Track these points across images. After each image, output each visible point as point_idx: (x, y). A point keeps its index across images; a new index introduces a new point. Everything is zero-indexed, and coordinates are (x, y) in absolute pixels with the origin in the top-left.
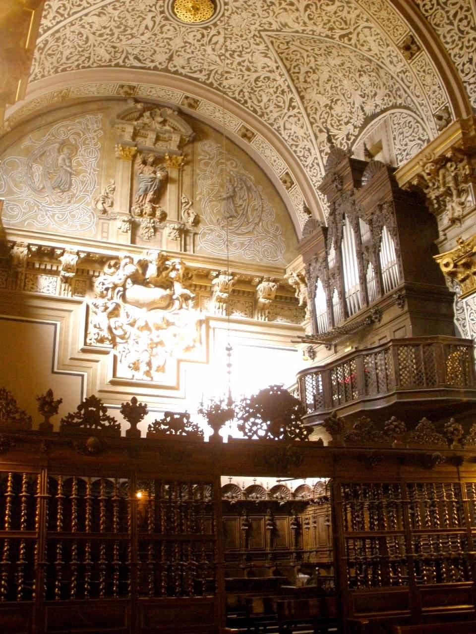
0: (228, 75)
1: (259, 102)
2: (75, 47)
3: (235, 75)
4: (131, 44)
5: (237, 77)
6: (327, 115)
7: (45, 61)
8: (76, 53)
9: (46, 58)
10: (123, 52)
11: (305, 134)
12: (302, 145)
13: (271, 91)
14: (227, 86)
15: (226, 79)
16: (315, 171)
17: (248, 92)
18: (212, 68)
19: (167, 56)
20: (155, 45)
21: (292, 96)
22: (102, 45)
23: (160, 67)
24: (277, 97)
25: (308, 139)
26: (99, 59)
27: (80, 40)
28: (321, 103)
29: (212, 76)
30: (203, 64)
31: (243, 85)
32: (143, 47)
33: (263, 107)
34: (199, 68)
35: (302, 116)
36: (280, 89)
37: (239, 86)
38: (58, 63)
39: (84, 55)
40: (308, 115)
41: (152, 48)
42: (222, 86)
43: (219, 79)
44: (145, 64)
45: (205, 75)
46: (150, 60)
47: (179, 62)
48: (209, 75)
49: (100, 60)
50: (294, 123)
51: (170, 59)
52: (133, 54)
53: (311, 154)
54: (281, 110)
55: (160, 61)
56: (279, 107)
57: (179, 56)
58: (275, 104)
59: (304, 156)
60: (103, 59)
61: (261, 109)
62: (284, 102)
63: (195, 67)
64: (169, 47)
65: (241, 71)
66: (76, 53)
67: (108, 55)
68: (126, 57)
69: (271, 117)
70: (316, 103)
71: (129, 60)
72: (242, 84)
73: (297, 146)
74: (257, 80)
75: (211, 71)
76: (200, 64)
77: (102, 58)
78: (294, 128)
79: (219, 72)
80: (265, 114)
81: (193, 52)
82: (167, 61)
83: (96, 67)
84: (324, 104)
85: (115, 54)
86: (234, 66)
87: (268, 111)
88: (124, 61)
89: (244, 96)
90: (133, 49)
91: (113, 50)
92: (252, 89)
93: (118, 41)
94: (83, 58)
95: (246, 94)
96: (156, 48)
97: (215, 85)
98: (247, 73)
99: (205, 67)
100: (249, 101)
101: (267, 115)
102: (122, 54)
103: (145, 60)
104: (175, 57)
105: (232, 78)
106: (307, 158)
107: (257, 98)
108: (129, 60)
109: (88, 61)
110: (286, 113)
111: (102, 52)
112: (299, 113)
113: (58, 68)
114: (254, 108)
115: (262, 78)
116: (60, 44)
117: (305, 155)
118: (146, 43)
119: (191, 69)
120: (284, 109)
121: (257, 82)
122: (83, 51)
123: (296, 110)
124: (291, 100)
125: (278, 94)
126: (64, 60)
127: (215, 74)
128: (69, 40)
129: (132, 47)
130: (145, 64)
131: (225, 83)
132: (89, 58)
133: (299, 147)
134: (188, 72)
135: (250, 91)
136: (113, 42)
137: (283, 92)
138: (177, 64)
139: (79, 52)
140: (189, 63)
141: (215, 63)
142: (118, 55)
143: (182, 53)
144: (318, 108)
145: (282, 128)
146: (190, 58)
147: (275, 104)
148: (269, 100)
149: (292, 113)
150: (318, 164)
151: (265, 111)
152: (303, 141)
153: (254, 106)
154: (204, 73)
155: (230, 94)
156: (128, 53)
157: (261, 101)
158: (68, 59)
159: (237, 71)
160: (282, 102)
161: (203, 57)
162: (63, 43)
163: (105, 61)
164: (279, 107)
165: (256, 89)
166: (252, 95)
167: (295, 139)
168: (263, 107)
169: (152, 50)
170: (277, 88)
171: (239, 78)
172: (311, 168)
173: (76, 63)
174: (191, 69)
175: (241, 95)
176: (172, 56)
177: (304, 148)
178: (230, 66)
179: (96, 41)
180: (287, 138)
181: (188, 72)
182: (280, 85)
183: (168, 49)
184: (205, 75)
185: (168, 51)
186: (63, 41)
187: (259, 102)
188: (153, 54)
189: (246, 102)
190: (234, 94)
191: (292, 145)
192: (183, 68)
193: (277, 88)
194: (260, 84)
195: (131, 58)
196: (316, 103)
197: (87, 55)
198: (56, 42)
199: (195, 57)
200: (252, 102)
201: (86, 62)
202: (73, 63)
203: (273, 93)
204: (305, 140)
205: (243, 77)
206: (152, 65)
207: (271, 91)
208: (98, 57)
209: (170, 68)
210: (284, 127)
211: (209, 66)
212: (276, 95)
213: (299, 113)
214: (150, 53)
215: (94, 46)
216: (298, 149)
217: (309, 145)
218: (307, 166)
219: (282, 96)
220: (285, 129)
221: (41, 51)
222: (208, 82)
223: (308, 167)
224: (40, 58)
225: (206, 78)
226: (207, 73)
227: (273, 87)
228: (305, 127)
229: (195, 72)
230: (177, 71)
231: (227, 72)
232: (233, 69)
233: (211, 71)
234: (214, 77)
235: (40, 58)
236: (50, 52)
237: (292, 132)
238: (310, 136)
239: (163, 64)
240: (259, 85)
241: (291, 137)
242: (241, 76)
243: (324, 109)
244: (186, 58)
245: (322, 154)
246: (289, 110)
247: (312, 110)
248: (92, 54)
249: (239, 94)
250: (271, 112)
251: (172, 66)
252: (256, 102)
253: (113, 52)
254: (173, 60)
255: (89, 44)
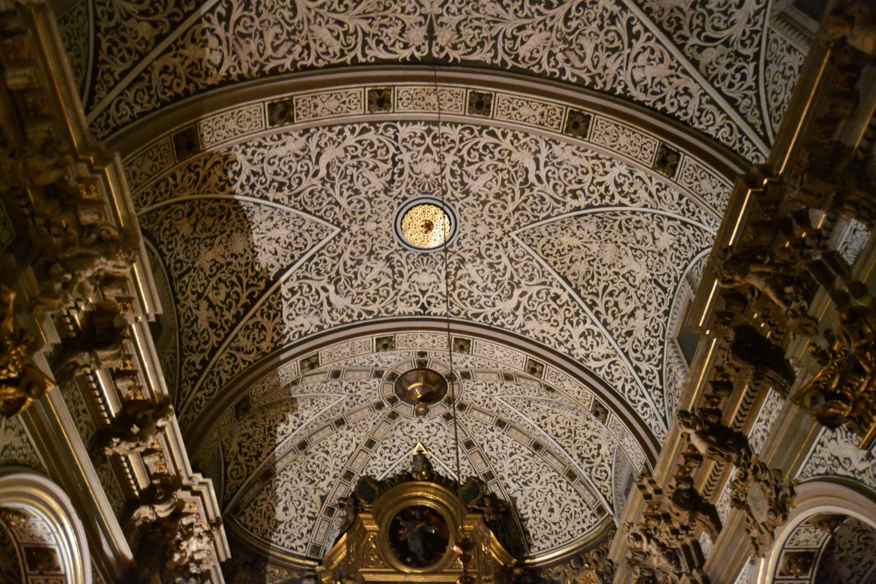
0: (523, 34)
1: (582, 60)
2: (279, 23)
3: (533, 28)
4: (364, 12)
5: (537, 30)
6: (701, 18)
7: (239, 50)
8: (285, 36)
9: (236, 40)
10: (356, 32)
11: (671, 67)
12: (669, 91)
13: (594, 26)
14: (528, 55)
15: (523, 43)
16: (710, 116)
17: (561, 51)
18: (494, 33)
19: (423, 31)
20: (400, 10)
21: (630, 15)
22: (319, 19)
23: (418, 55)
24: (606, 34)
25: (679, 73)
26: (323, 49)
27: (283, 7)
28: (683, 6)
29: (500, 47)
30: (480, 28)
31: (550, 42)
32: (384, 17)
33: (591, 67)
34: (478, 40)
35: (658, 41)
36: (606, 15)
37: (544, 47)
38: (261, 55)
39: (298, 42)
40: (669, 35)
41: (397, 18)
42: (520, 59)
43: (511, 49)
44: (395, 53)
45: (489, 51)
46: (402, 45)
47: (444, 36)
48: (495, 47)
49: (327, 53)
50: (644, 63)
51: (431, 37)
52: (374, 35)
53: (691, 95)
54: (620, 55)
55: (417, 44)
56: (614, 50)
57: (442, 24)
58: (608, 49)
59: (680, 108)
60: (331, 50)
61: (589, 71)
62: (620, 37)
63: (471, 40)
64: (423, 11)
65: (540, 13)
66: (285, 36)
67: (334, 41)
68: (365, 43)
69: (608, 80)
70: (675, 10)
71: (370, 48)
72: (548, 39)
73: (663, 100)
74: (567, 19)
75: (496, 38)
76: (478, 31)
77: (327, 48)
78: (650, 71)
79: (509, 35)
80: (597, 79)
81: (460, 10)
82: (427, 42)
83: (326, 67)
84: (689, 5)
85: (345, 39)
86: (526, 11)
87: (600, 70)
88: (364, 55)
89: (557, 63)
90: (370, 25)
91: (341, 29)
92: (565, 41)
93: (342, 9)
94: (298, 49)
95: (560, 57)
96: (402, 16)
97: (510, 63)
98: (551, 12)
99: (485, 33)
100: (567, 67)
101: (601, 77)
102: (356, 38)
103: (393, 45)
104: (438, 31)
105: (529, 36)
106: (686, 108)
107: (576, 54)
108: (370, 48)
109: (309, 55)
110: (629, 55)
111: (323, 33)
112: (649, 39)
113: (263, 66)
114: (579, 78)
115: (574, 12)
116: (253, 14)
117: (683, 105)
118: (386, 8)
119: (467, 47)
120: (623, 49)
121: (569, 23)
122: (294, 32)
123: (643, 37)
124: (629, 27)
125: (606, 28)
126: (269, 51)
127: (504, 42)
128: (265, 6)
129: (367, 18)
130: (395, 53)
131: (523, 51)
132: (307, 47)
133: (668, 98)
134: (465, 54)
135: (563, 47)
136: (335, 11)
137: (613, 19)
138: (443, 44)
139: (288, 34)
140: (461, 36)
141: (496, 20)
142: (352, 40)
143: (445, 18)
144: (681, 16)
145: (631, 87)
146: (459, 24)
147: (608, 49)
148: (596, 49)
149: (638, 45)
150: (712, 102)
151: (594, 72)
152: (670, 83)
153: (577, 72)
154: (488, 46)
155: (535, 69)
156: (365, 34)
157: (585, 57)
158: (275, 49)
159: (533, 17)
160: (616, 39)
161: (476, 15)
162: (259, 14)
163: (335, 55)
164: (614, 50)
165: (571, 37)
166: (568, 53)
167: (657, 90)
168: (591, 67)
169: (400, 23)
170: (602, 16)
171: (540, 31)
172: (699, 118)
173: (290, 58)
174: (467, 47)
175: (553, 63)
176: (431, 30)
177: (677, 93)
178: (520, 14)
179: (309, 9)
180: (641, 97)
181: (465, 54)
182: (605, 9)
183: (421, 14)
184: (489, 51)
185: (422, 19)
186: (257, 8)
187: (582, 60)
188: (403, 30)
189: (563, 71)
190: (540, 67)
191: (654, 103)
192: (455, 47)
193: (602, 16)
194: (573, 24)
195: (372, 42)
196: (675, 10)
197: (304, 43)
198: (246, 9)
199: (465, 20)
200: (573, 66)
201: (305, 55)
202: (284, 57)
203: (597, 30)
204: (674, 80)
205: (545, 25)
206: (406, 54)
207: (594, 26)
208: (321, 45)
209: (435, 55)
210: (633, 80)
211: (491, 28)
212: (604, 31)
213: (649, 39)
214: (398, 29)
215: (309, 20)
216: (667, 104)
217: (683, 82)
218: (691, 120)
219: (613, 28)
220: (635, 84)
221: (224, 23)
222: (498, 61)
223: (695, 120)
224: (227, 39)
225: (492, 54)
226: (492, 43)
227: (595, 19)
228: (667, 56)
229: (475, 49)
230: (447, 56)
231: (521, 28)
232: (527, 17)
233: (496, 38)
234: (504, 48)
235: (227, 39)
236: (240, 28)
237: (649, 81)
238: (679, 64)
239: (422, 48)
240: (572, 29)
241: (650, 90)
242: (541, 26)
243: (692, 12)
244: (454, 27)
245: (715, 83)
246: (630, 46)
247: (672, 24)
248: (310, 38)
249: (549, 62)
250: (605, 68)
251: (438, 49)
252: (578, 64)
253: (342, 36)
254: (435, 38)
255: (299, 17)
